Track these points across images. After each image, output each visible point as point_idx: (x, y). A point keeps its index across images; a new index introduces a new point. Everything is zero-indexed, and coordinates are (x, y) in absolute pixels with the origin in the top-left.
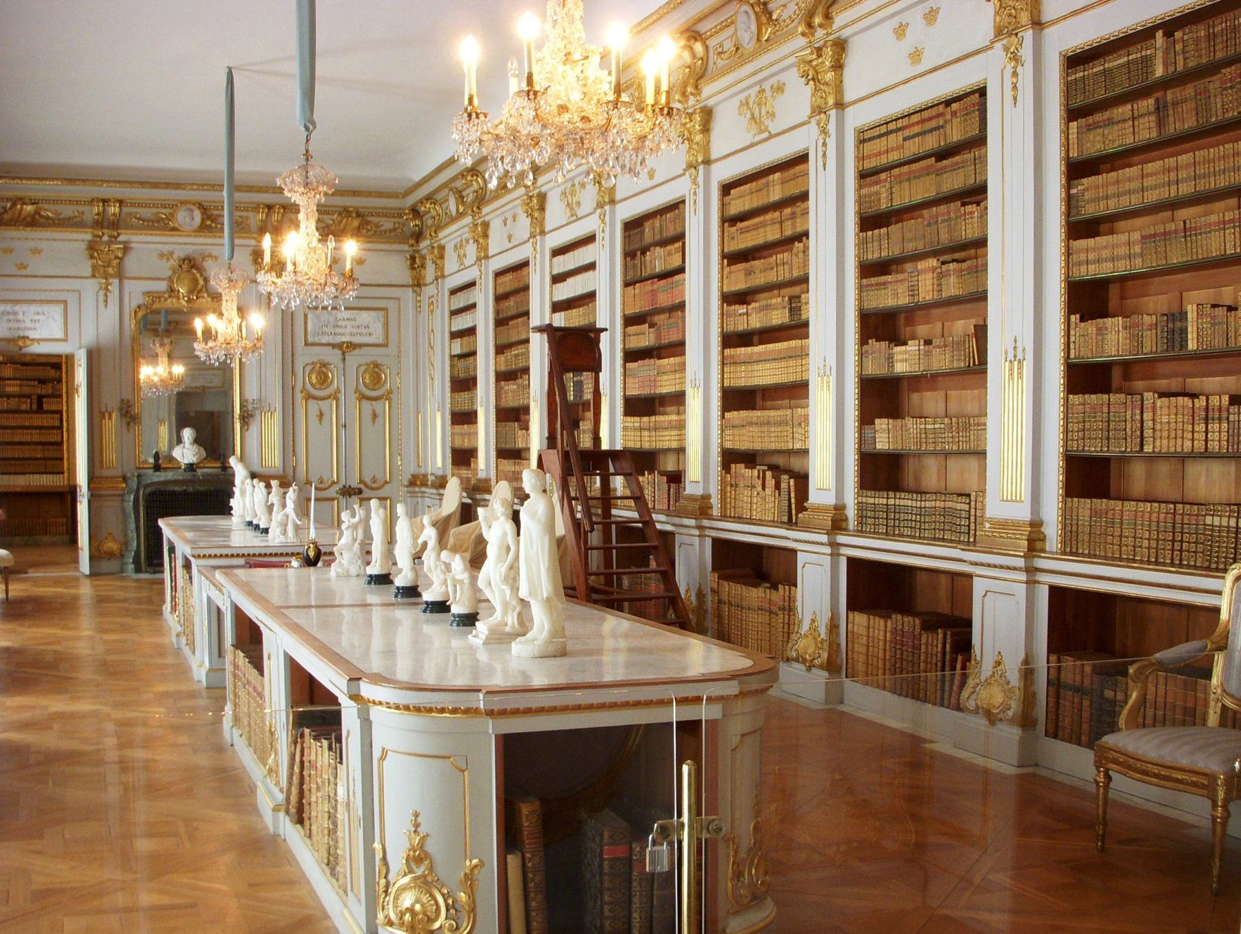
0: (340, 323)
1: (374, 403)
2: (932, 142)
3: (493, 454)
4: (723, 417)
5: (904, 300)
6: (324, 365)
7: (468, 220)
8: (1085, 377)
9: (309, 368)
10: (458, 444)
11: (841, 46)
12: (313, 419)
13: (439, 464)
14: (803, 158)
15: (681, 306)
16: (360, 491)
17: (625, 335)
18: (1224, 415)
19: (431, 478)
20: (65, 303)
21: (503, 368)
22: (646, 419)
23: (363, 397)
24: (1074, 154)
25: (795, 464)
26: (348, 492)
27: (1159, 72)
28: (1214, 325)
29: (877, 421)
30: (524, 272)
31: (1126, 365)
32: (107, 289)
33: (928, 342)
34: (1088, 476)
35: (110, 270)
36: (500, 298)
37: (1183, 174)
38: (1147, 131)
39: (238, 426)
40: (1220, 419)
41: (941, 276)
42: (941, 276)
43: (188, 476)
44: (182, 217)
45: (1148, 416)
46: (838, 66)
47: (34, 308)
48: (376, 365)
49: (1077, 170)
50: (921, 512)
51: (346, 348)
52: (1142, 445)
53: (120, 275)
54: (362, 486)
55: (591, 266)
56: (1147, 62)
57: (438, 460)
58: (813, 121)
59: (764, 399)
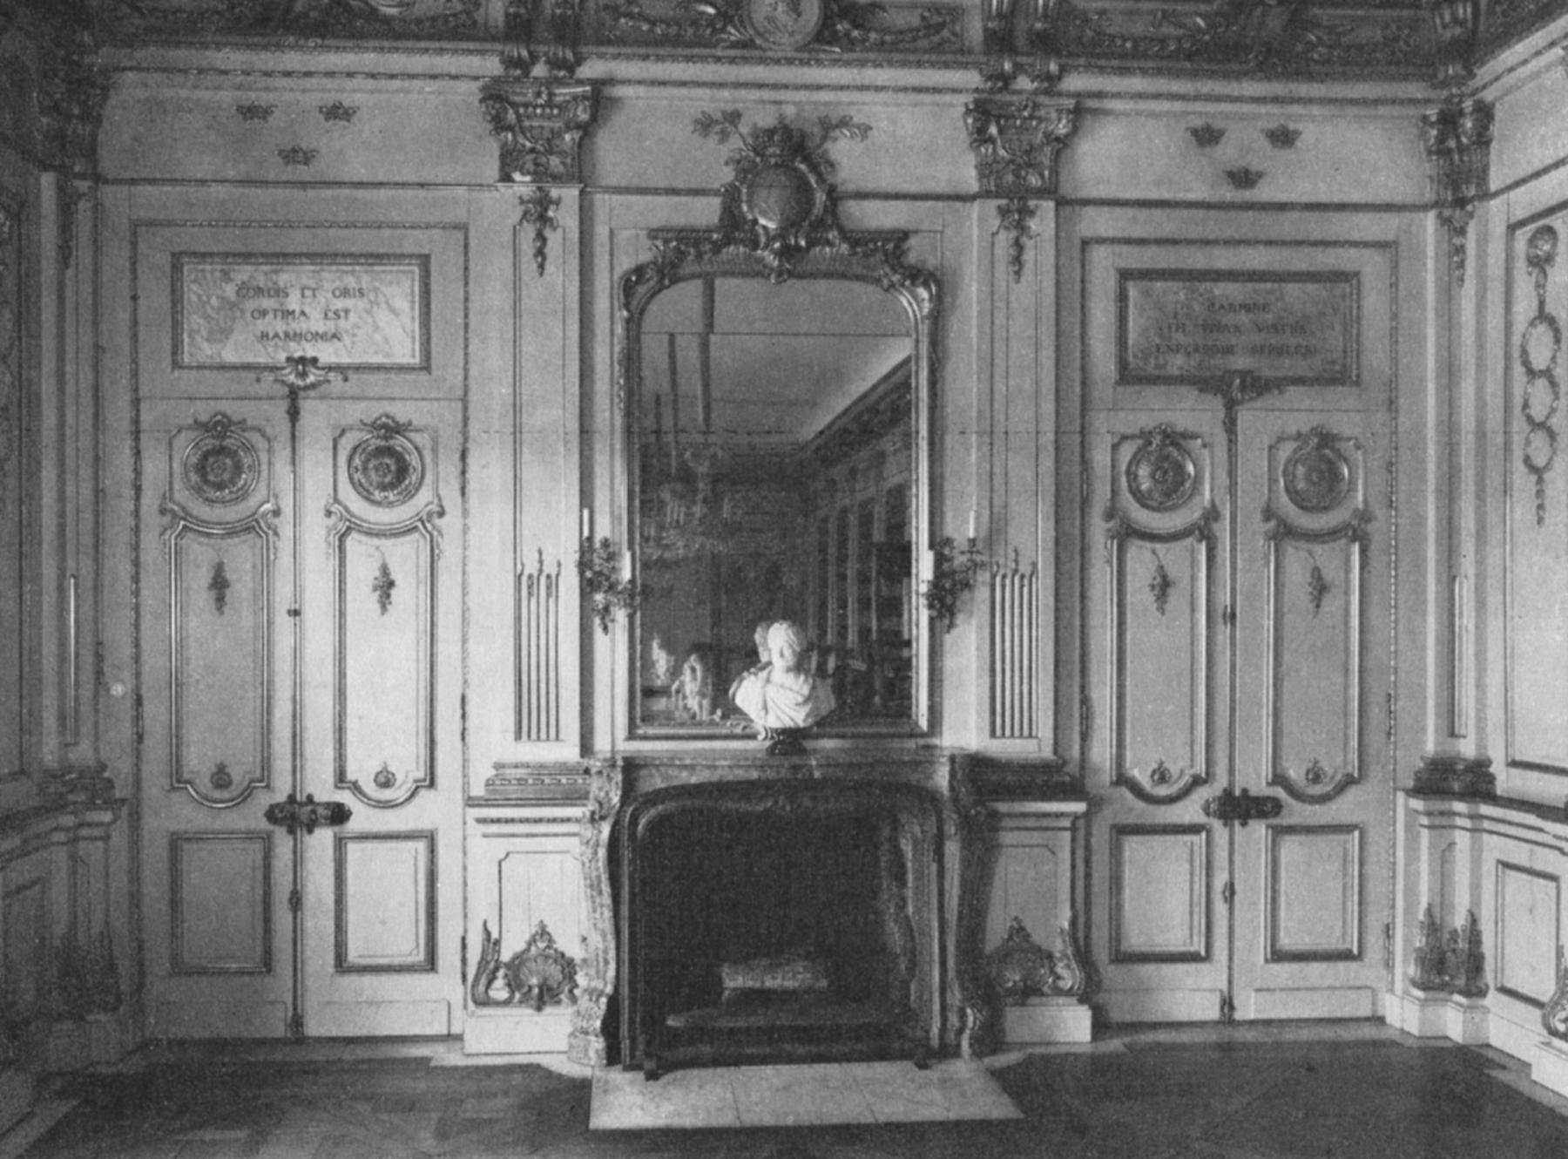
0: (1229, 319)
1: (1318, 549)
9: (1127, 452)
16: (1276, 807)
20: (425, 261)
23: (1284, 533)
26: (1238, 807)
32: (543, 219)
35: (555, 161)
39: (924, 616)
43: (780, 770)
47: (331, 277)
53: (581, 173)
54: (1279, 792)
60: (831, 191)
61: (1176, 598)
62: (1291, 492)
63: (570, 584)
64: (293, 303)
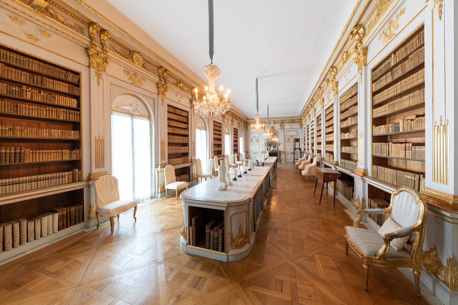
2: (350, 96)
8: (377, 139)
11: (337, 83)
18: (410, 148)
24: (374, 90)
27: (392, 64)
28: (407, 125)
31: (391, 136)
37: (398, 88)
38: (389, 80)
40: (409, 150)
41: (351, 120)
42: (351, 120)
44: (271, 122)
45: (390, 148)
46: (337, 86)
49: (374, 94)
50: (349, 164)
51: (292, 136)
52: (389, 155)
56: (389, 63)
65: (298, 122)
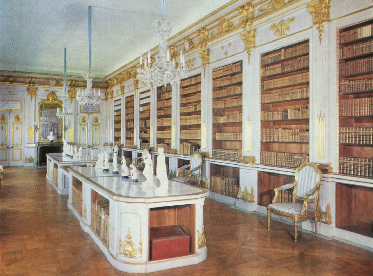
3: (125, 138)
4: (180, 131)
5: (223, 107)
6: (84, 117)
7: (119, 85)
9: (81, 118)
10: (116, 136)
12: (82, 129)
13: (111, 140)
14: (200, 75)
15: (171, 106)
17: (157, 113)
19: (109, 144)
21: (127, 119)
22: (162, 132)
25: (198, 143)
26: (89, 147)
27: (282, 58)
29: (217, 134)
30: (133, 97)
33: (228, 116)
34: (266, 146)
35: (33, 94)
36: (127, 103)
48: (97, 117)
49: (263, 79)
53: (35, 94)
55: (149, 97)
56: (280, 56)
57: (111, 140)
58: (202, 67)
59: (189, 127)
60: (56, 97)
61: (84, 129)
62: (94, 122)
63: (33, 128)
64: (9, 104)
65: (101, 88)
